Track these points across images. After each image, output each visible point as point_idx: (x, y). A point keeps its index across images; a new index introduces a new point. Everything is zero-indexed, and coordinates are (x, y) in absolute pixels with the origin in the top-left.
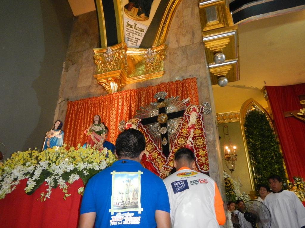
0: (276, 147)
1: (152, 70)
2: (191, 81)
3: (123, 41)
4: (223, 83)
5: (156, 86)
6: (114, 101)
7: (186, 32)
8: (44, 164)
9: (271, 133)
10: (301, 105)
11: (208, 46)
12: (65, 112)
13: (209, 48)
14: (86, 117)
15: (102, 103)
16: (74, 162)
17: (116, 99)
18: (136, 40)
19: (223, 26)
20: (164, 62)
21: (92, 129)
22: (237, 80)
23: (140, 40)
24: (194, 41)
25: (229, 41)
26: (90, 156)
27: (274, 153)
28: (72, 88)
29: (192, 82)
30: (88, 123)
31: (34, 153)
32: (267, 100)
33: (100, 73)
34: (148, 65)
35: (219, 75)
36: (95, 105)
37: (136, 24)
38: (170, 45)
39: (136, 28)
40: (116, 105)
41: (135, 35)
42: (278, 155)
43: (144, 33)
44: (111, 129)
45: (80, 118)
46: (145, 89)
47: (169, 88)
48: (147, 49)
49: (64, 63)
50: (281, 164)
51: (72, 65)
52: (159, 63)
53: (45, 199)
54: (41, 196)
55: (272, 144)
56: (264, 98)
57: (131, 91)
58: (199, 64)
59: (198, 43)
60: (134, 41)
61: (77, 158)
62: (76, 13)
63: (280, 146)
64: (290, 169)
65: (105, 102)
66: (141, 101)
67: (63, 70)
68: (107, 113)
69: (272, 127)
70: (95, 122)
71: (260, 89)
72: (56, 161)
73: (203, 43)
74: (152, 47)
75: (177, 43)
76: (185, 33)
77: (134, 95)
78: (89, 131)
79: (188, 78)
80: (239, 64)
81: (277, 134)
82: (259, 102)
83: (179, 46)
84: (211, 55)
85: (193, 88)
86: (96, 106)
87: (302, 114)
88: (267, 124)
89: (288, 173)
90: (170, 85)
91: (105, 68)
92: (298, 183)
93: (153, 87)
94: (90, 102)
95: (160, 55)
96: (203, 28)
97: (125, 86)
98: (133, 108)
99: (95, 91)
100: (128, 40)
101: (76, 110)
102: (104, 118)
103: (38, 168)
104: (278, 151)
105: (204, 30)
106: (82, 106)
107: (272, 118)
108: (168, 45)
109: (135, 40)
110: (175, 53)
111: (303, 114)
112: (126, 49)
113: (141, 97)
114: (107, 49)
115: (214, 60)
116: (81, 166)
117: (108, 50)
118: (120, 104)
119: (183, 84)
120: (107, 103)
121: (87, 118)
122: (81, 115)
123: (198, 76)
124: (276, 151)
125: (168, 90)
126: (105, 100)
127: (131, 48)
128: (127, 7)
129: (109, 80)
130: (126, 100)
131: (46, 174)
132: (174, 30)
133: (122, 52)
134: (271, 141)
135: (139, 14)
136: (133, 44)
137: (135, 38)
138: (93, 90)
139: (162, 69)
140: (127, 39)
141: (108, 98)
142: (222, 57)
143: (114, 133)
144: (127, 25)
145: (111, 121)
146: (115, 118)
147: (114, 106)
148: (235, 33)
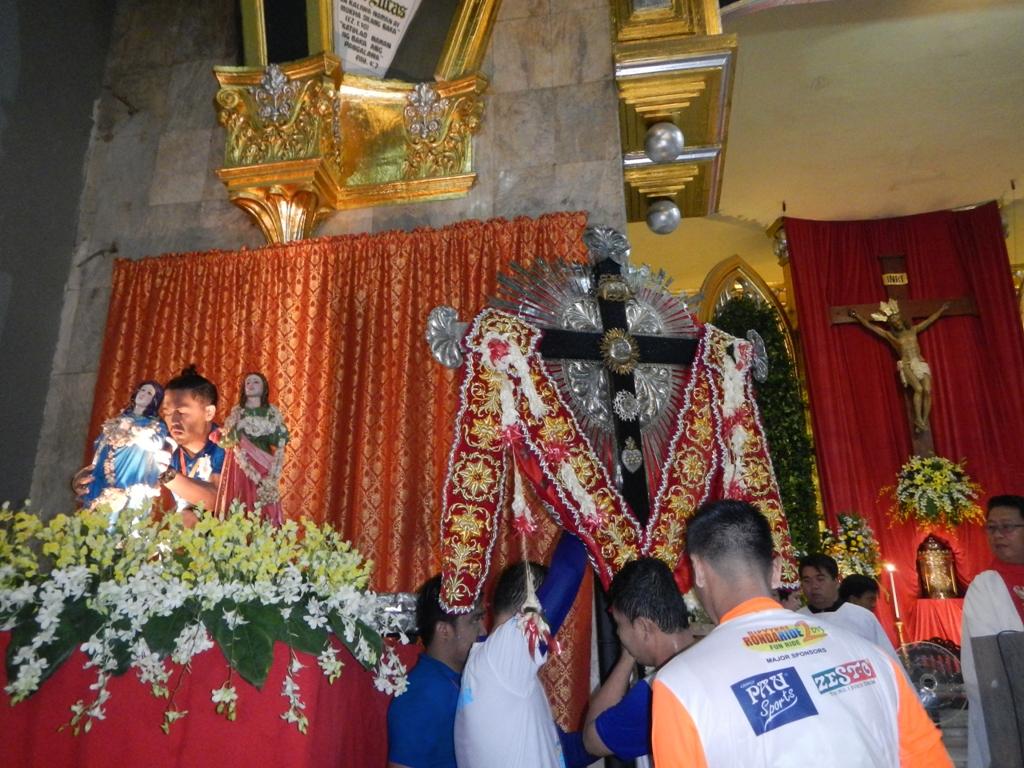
0: (796, 418)
1: (431, 167)
2: (568, 222)
3: (326, 47)
4: (665, 221)
5: (446, 229)
6: (292, 270)
7: (557, 36)
8: (71, 579)
9: (786, 374)
10: (886, 287)
11: (630, 96)
12: (102, 299)
13: (634, 106)
14: (186, 326)
15: (245, 274)
16: (186, 575)
17: (299, 266)
18: (375, 44)
19: (687, 30)
20: (474, 141)
21: (238, 428)
22: (709, 213)
23: (389, 46)
24: (584, 74)
25: (701, 85)
26: (243, 550)
27: (790, 437)
28: (129, 206)
29: (572, 227)
30: (194, 349)
31: (21, 520)
32: (782, 264)
33: (240, 164)
34: (418, 147)
35: (653, 195)
36: (220, 283)
38: (496, 77)
40: (299, 288)
41: (372, 27)
42: (799, 445)
43: (404, 20)
44: (281, 375)
45: (164, 326)
46: (407, 238)
47: (492, 243)
48: (417, 87)
49: (97, 103)
50: (806, 472)
51: (128, 117)
52: (457, 142)
53: (88, 727)
54: (75, 713)
55: (786, 408)
56: (776, 257)
57: (355, 242)
58: (595, 163)
59: (598, 81)
60: (368, 49)
61: (194, 558)
63: (808, 415)
64: (831, 486)
65: (258, 274)
66: (390, 280)
67: (94, 132)
68: (264, 313)
69: (791, 352)
70: (250, 399)
71: (767, 225)
72: (116, 563)
73: (615, 84)
74: (434, 80)
75: (522, 73)
76: (553, 37)
77: (364, 254)
78: (229, 435)
79: (558, 213)
80: (723, 162)
81: (803, 378)
82: (754, 267)
83: (532, 86)
84: (638, 129)
85: (574, 250)
86: (223, 283)
87: (884, 319)
88: (777, 344)
89: (823, 501)
90: (495, 231)
91: (259, 146)
92: (852, 534)
93: (434, 231)
94: (201, 268)
95: (464, 114)
96: (616, 29)
97: (332, 216)
98: (360, 303)
99: (217, 225)
100: (347, 44)
101: (148, 294)
102: (253, 332)
103: (49, 593)
104: (801, 432)
105: (621, 36)
106: (169, 283)
107: (795, 326)
108: (492, 76)
109: (372, 46)
110: (516, 112)
111: (889, 317)
112: (338, 78)
113: (390, 267)
114: (269, 74)
115: (646, 146)
116: (214, 591)
117: (271, 79)
118: (314, 284)
119: (540, 230)
120: (266, 279)
121: (192, 329)
122: (166, 316)
123: (593, 204)
124: (797, 432)
125: (486, 249)
126: (259, 265)
127: (355, 73)
129: (273, 191)
130: (338, 271)
131: (80, 619)
132: (514, 23)
133: (325, 92)
134: (783, 398)
136: (364, 61)
137: (373, 39)
138: (211, 222)
139: (468, 165)
140: (342, 40)
141: (268, 260)
142: (672, 141)
143: (290, 391)
145: (280, 347)
146: (295, 335)
147: (293, 291)
148: (727, 61)
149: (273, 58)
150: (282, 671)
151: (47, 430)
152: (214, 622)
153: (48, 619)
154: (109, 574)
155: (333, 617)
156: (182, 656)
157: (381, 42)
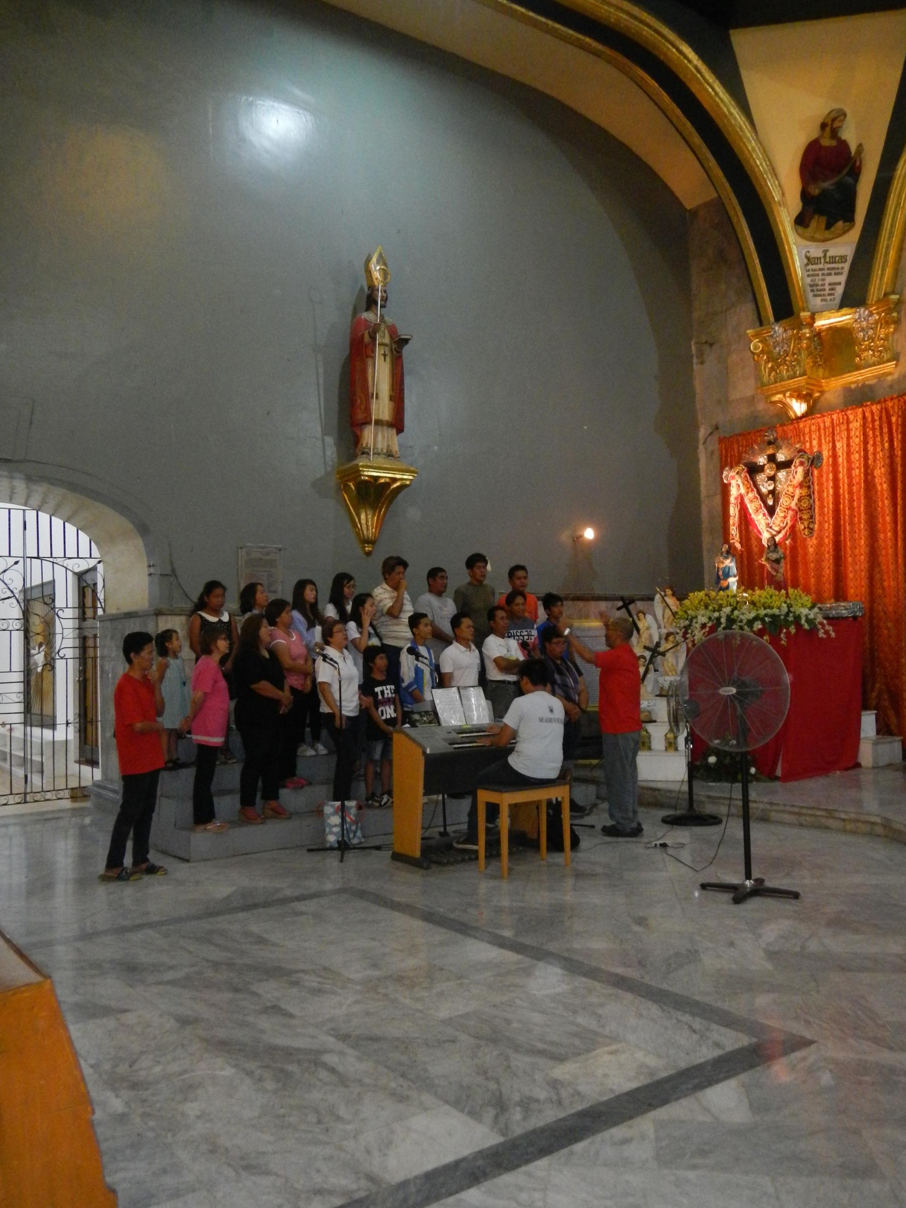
23: (840, 284)
37: (825, 252)
39: (828, 260)
49: (693, 343)
60: (827, 292)
62: (689, 205)
67: (695, 360)
116: (762, 612)
118: (815, 443)
128: (801, 221)
131: (731, 621)
135: (828, 226)
137: (830, 284)
138: (761, 406)
144: (806, 261)
149: (778, 319)
150: (780, 632)
151: (705, 525)
152: (762, 620)
153: (723, 620)
154: (735, 608)
155: (797, 618)
156: (755, 629)
157: (835, 284)
